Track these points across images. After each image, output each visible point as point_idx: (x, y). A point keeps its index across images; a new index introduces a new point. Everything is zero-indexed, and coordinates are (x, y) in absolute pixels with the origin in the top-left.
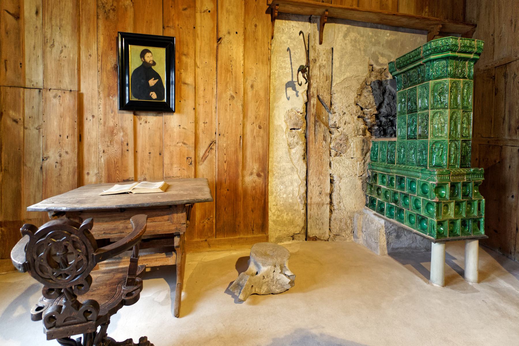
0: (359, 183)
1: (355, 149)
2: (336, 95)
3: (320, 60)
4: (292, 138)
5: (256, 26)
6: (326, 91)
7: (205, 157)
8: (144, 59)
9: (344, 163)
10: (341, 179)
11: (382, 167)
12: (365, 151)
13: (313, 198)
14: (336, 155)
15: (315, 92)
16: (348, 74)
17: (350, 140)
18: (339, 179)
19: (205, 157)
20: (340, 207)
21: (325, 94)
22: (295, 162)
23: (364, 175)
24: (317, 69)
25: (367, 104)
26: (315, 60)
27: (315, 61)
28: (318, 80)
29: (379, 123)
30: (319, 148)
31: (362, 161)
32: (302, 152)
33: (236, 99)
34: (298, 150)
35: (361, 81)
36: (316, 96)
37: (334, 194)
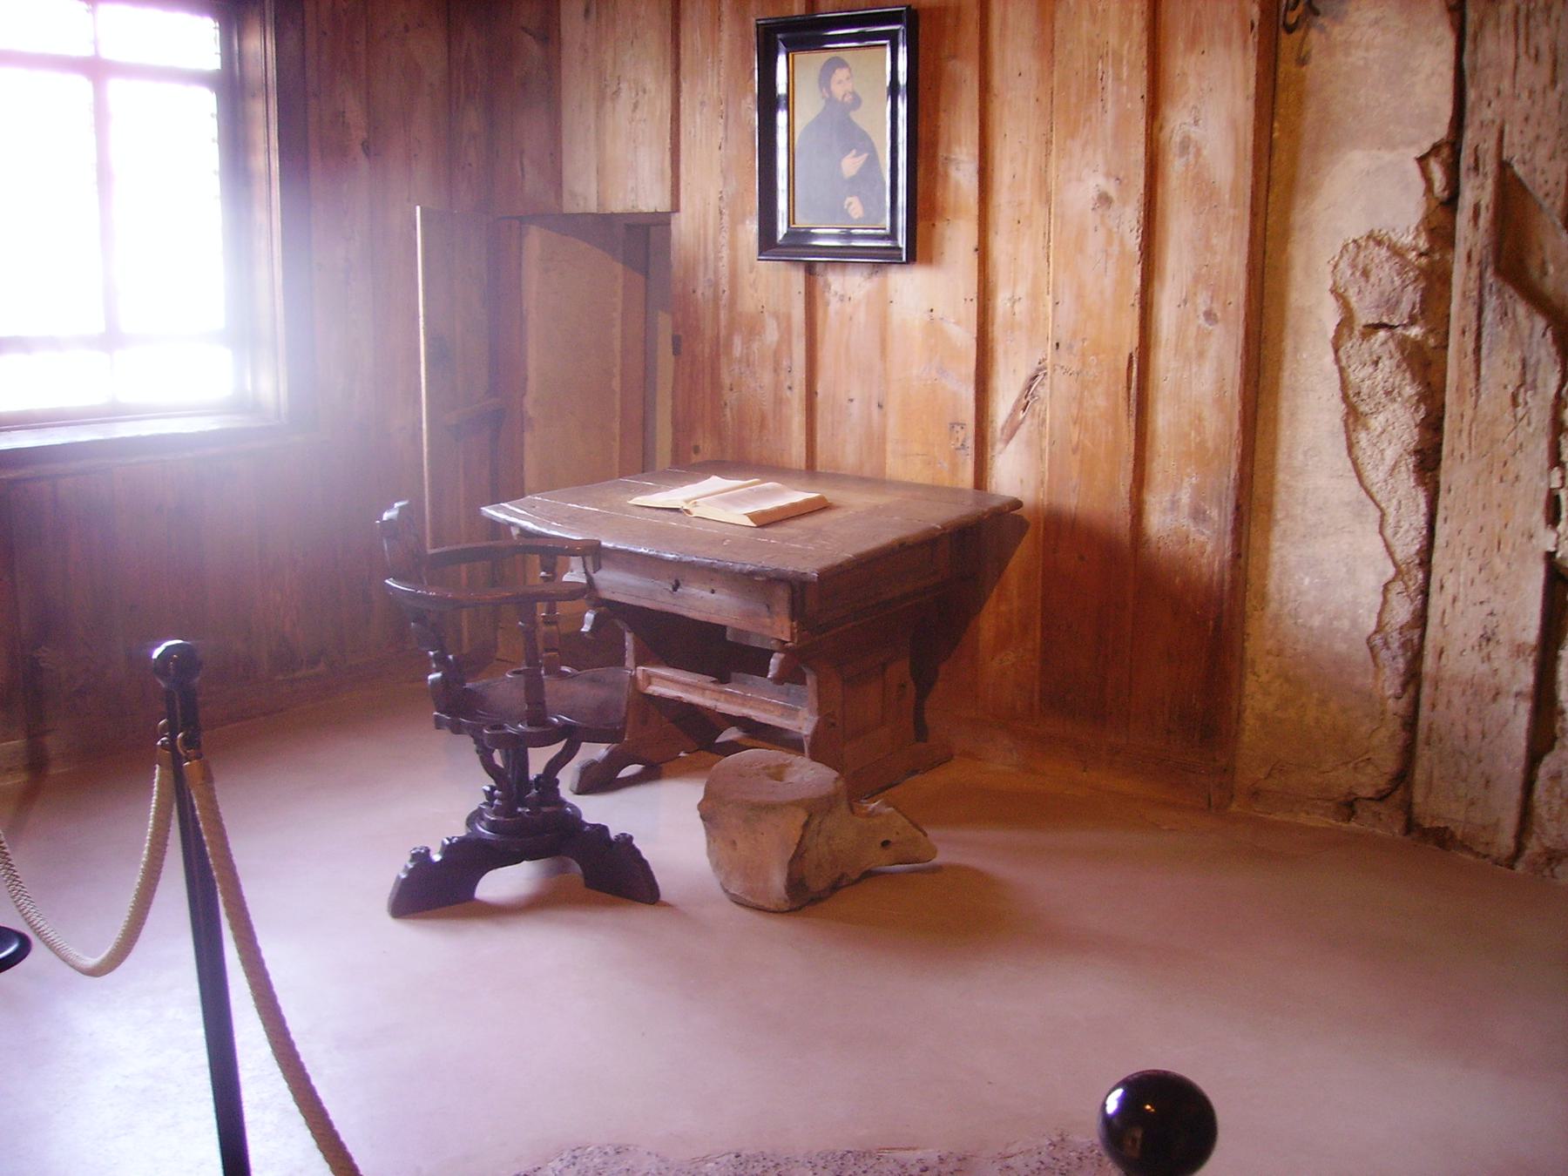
4: (1371, 370)
7: (1012, 429)
8: (830, 92)
13: (1451, 653)
15: (1490, 145)
19: (1012, 429)
21: (1542, 152)
22: (1375, 476)
28: (1506, 85)
33: (1116, 205)
34: (1394, 428)
36: (1490, 166)
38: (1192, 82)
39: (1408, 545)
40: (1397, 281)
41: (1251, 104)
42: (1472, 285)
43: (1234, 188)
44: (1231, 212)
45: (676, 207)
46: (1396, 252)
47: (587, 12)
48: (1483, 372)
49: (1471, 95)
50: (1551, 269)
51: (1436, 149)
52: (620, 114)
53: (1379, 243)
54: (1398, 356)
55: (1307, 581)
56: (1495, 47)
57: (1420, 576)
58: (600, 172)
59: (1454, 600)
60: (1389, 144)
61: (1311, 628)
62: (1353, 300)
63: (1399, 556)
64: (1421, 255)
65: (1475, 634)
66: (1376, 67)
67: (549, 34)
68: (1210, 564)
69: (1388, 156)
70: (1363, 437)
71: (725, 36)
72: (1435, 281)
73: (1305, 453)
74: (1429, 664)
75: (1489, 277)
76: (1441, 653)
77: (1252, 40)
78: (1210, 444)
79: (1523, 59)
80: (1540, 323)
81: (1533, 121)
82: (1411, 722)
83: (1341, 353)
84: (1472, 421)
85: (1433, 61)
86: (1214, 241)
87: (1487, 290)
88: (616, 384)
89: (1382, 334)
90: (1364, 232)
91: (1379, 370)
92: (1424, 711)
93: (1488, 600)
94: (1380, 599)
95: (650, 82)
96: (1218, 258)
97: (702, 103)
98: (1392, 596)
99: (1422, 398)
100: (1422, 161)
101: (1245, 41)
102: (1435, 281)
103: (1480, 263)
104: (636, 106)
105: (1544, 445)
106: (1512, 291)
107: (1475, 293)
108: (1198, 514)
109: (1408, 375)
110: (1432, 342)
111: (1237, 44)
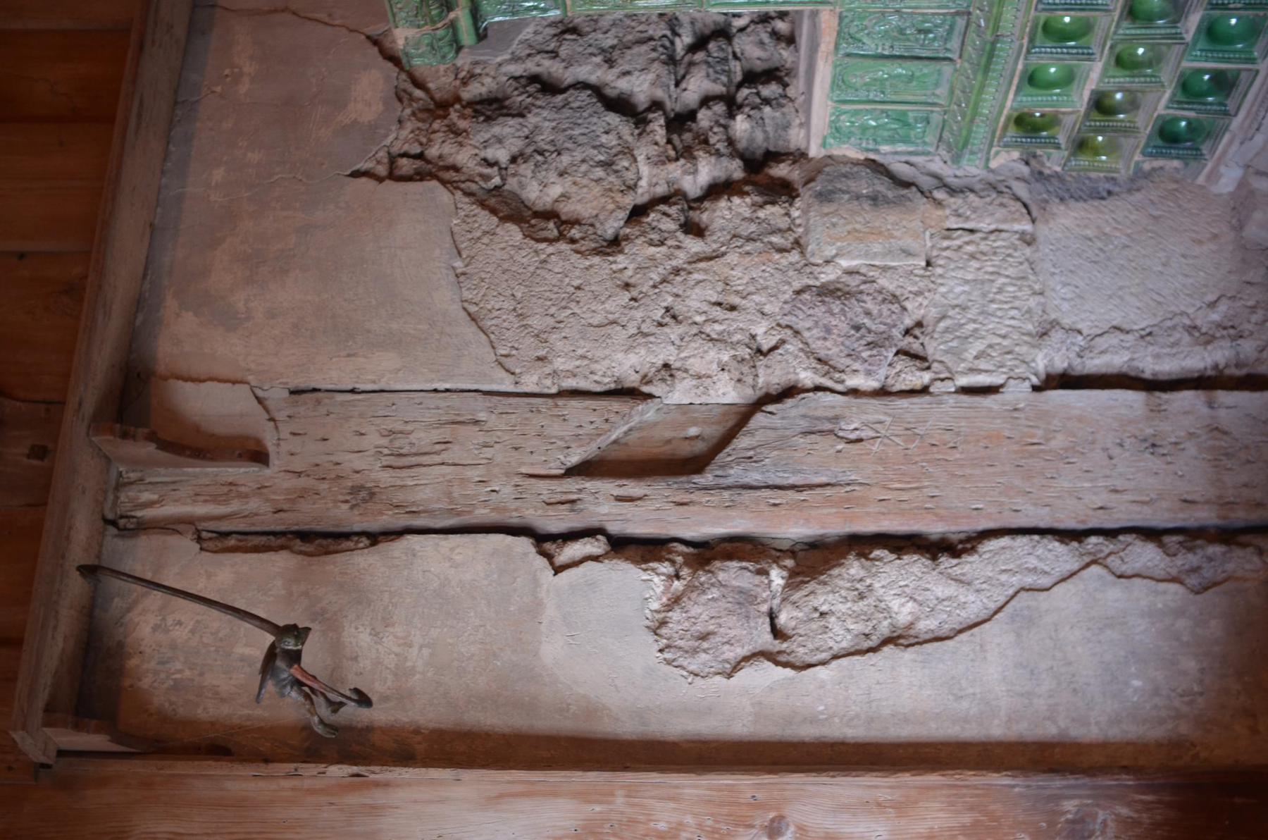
0: (1066, 221)
1: (877, 248)
2: (560, 363)
6: (538, 420)
9: (964, 308)
10: (1055, 324)
11: (982, 87)
12: (882, 186)
14: (918, 358)
16: (445, 299)
17: (828, 275)
18: (1057, 335)
20: (1220, 326)
21: (556, 429)
22: (975, 605)
23: (1021, 189)
24: (406, 478)
25: (612, 178)
26: (355, 490)
27: (364, 494)
28: (475, 474)
29: (720, 108)
30: (881, 460)
31: (939, 204)
32: (915, 564)
35: (486, 220)
36: (572, 484)
37: (1151, 364)
39: (1060, 556)
40: (714, 593)
41: (468, 775)
43: (583, 796)
44: (620, 800)
46: (675, 601)
48: (824, 480)
49: (482, 515)
50: (693, 431)
51: (549, 557)
53: (663, 623)
54: (812, 586)
55: (1137, 683)
56: (427, 490)
57: (1093, 539)
59: (1116, 491)
60: (535, 610)
61: (1202, 671)
62: (742, 651)
63: (1076, 566)
64: (678, 577)
65: (1154, 463)
66: (434, 633)
68: (1147, 807)
69: (550, 612)
70: (926, 625)
73: (958, 698)
74: (1205, 516)
75: (707, 478)
76: (1185, 501)
78: (967, 819)
79: (445, 457)
81: (518, 442)
83: (814, 660)
84: (885, 487)
86: (662, 826)
87: (721, 481)
89: (783, 619)
90: (651, 638)
91: (839, 605)
93: (1105, 450)
94: (1137, 581)
96: (689, 819)
98: (1125, 569)
99: (863, 555)
100: (558, 570)
101: (377, 784)
103: (687, 490)
105: (903, 403)
106: (722, 455)
107: (726, 494)
109: (835, 572)
110: (789, 563)
111: (379, 797)
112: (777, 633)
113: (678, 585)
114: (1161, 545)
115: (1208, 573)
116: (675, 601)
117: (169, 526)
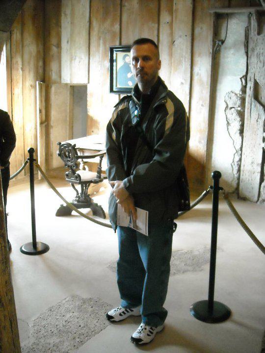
3: (258, 48)
5: (202, 28)
15: (253, 76)
27: (253, 50)
34: (236, 125)
36: (253, 80)
38: (199, 62)
39: (238, 147)
42: (250, 100)
45: (89, 83)
46: (236, 94)
47: (68, 42)
49: (249, 68)
51: (243, 77)
52: (76, 63)
53: (233, 93)
56: (253, 60)
57: (240, 152)
58: (71, 75)
67: (59, 46)
71: (101, 49)
72: (243, 100)
75: (253, 99)
77: (211, 55)
80: (261, 107)
82: (239, 179)
85: (243, 61)
88: (68, 119)
89: (233, 109)
92: (241, 176)
95: (83, 57)
97: (95, 62)
99: (241, 121)
100: (241, 79)
102: (243, 100)
104: (80, 62)
108: (200, 142)
112: (231, 108)
113: (239, 95)
114: (238, 161)
115: (234, 166)
116: (236, 94)
117: (250, 23)
